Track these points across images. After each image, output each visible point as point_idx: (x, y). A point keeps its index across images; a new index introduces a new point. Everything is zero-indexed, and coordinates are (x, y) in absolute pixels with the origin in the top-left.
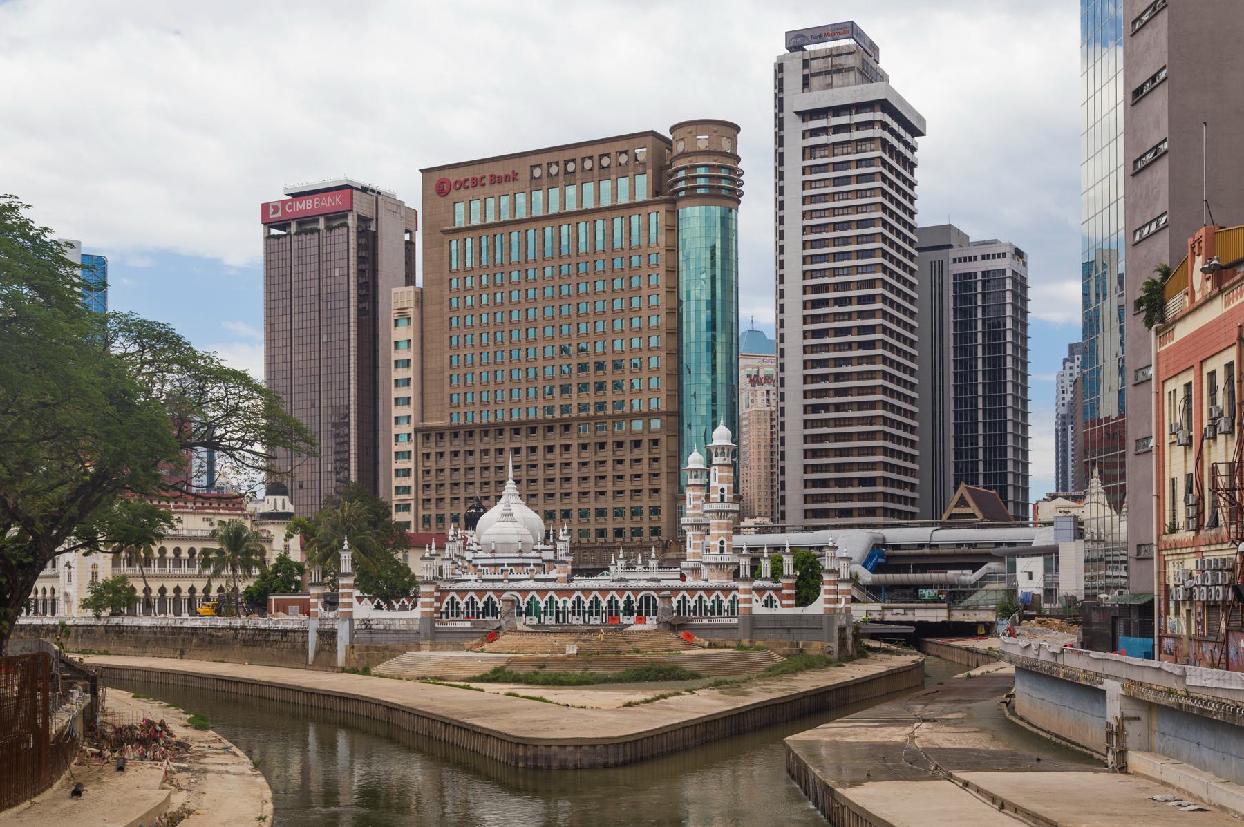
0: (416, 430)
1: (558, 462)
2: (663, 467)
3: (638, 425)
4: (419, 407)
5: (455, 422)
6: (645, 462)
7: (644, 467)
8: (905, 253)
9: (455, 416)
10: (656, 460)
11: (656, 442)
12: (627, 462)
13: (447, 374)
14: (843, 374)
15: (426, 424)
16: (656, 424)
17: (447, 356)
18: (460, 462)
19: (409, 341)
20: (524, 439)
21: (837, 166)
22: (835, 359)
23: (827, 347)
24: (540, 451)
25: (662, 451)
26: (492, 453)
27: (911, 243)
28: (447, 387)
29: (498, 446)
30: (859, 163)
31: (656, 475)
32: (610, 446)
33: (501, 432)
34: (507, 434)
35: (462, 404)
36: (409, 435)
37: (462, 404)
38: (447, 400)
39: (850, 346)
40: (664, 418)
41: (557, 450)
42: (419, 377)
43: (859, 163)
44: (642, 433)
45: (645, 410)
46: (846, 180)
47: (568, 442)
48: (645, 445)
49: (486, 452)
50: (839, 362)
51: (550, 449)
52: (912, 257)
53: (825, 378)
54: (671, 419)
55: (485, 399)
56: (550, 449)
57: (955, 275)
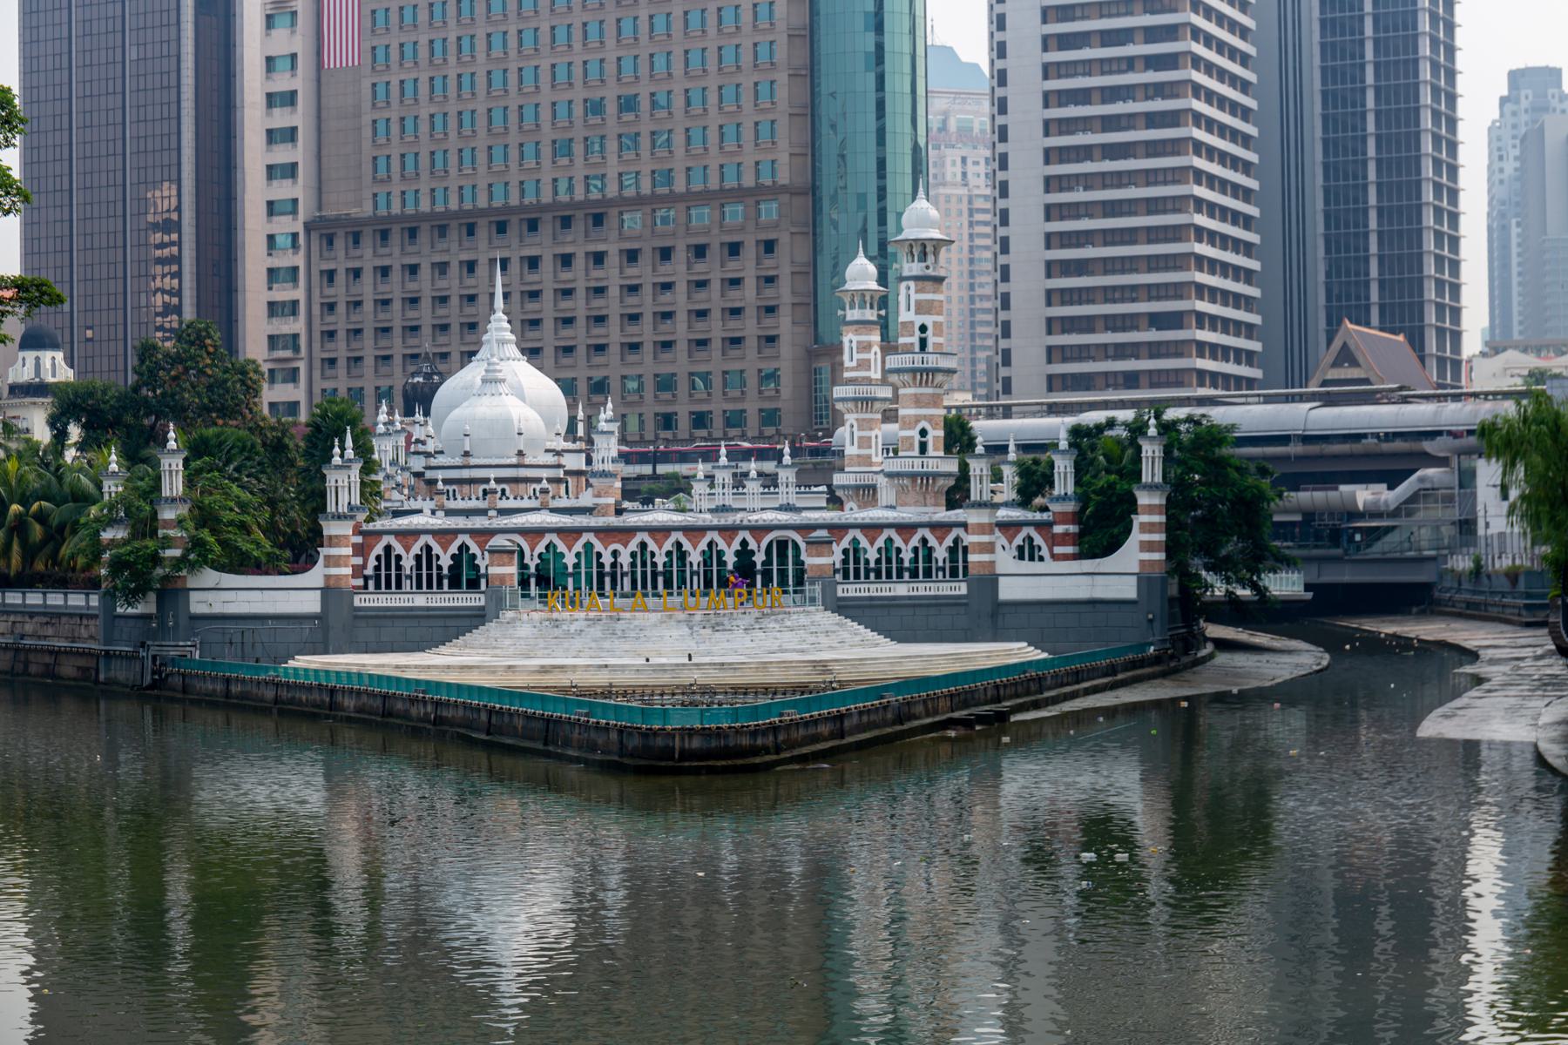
0: (309, 227)
1: (581, 286)
2: (784, 293)
3: (735, 213)
4: (314, 184)
5: (382, 211)
6: (750, 284)
7: (748, 295)
9: (382, 200)
10: (770, 280)
11: (769, 246)
12: (716, 286)
13: (367, 119)
14: (1119, 117)
15: (329, 212)
16: (770, 210)
17: (366, 85)
18: (395, 287)
19: (294, 56)
20: (515, 242)
22: (1102, 89)
23: (1087, 67)
24: (547, 265)
25: (783, 265)
26: (454, 269)
28: (367, 145)
29: (465, 257)
31: (771, 310)
32: (680, 255)
33: (471, 231)
34: (482, 233)
35: (396, 176)
36: (295, 236)
37: (396, 176)
38: (367, 168)
39: (1130, 64)
40: (785, 198)
41: (579, 263)
42: (312, 122)
44: (742, 229)
45: (748, 181)
47: (601, 247)
48: (750, 252)
49: (442, 268)
51: (566, 260)
53: (1084, 124)
54: (798, 201)
55: (439, 164)
56: (566, 260)
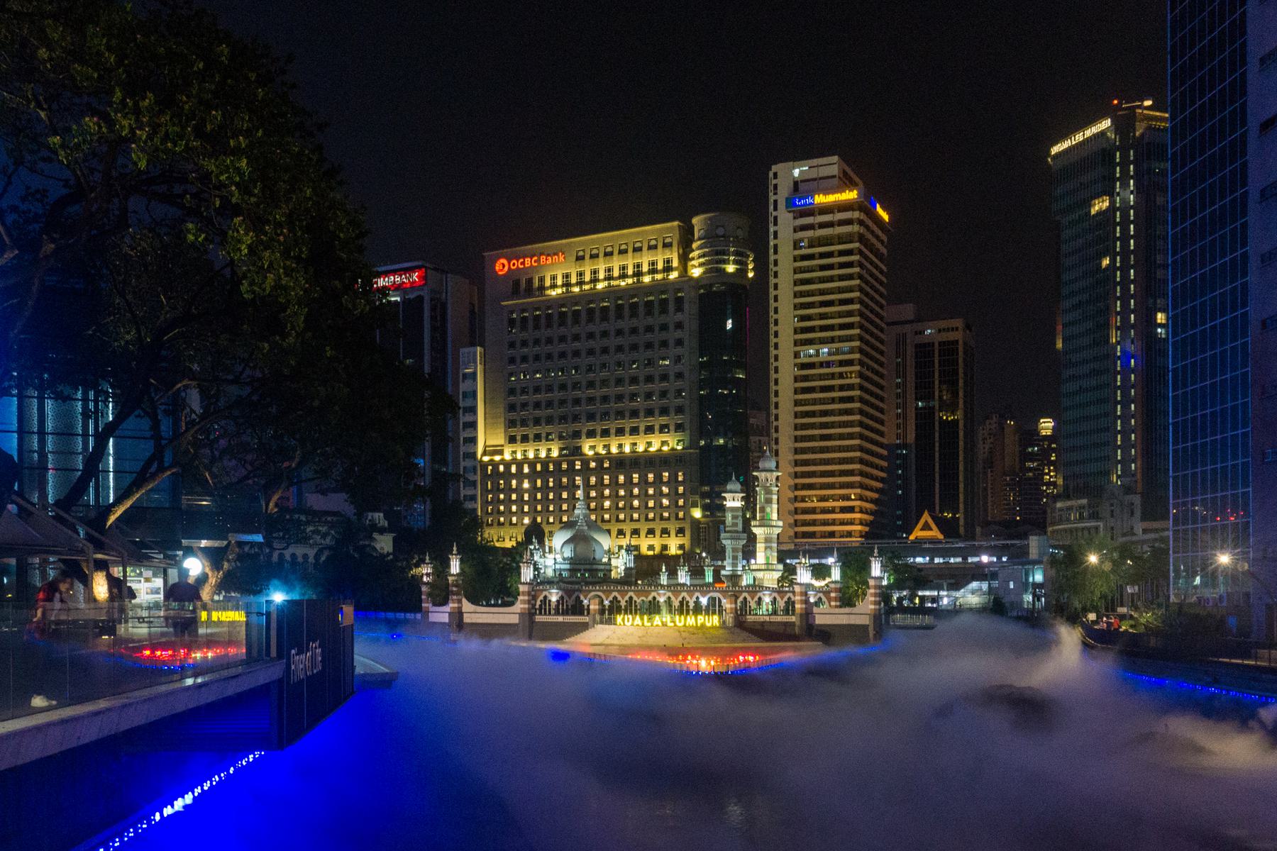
8: (877, 327)
21: (822, 256)
23: (815, 402)
27: (881, 318)
30: (841, 253)
43: (841, 253)
46: (831, 267)
50: (825, 413)
52: (882, 330)
53: (812, 426)
57: (916, 346)
